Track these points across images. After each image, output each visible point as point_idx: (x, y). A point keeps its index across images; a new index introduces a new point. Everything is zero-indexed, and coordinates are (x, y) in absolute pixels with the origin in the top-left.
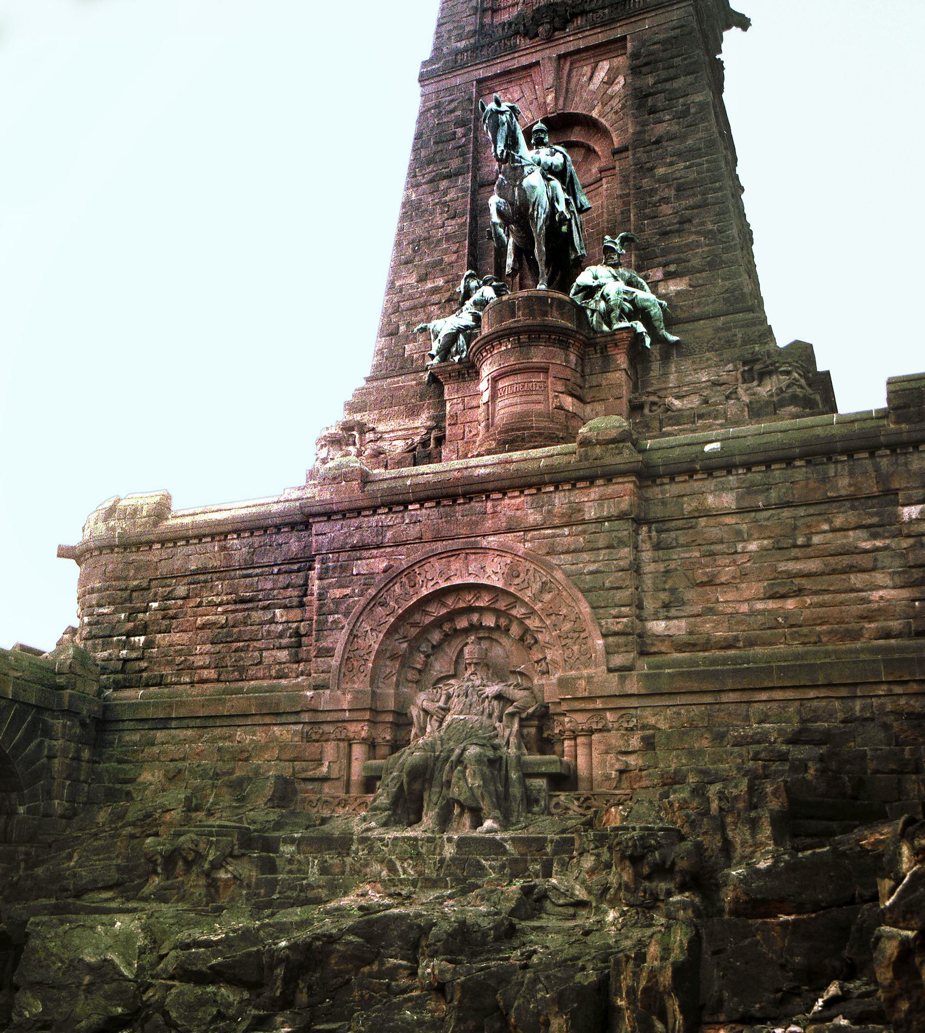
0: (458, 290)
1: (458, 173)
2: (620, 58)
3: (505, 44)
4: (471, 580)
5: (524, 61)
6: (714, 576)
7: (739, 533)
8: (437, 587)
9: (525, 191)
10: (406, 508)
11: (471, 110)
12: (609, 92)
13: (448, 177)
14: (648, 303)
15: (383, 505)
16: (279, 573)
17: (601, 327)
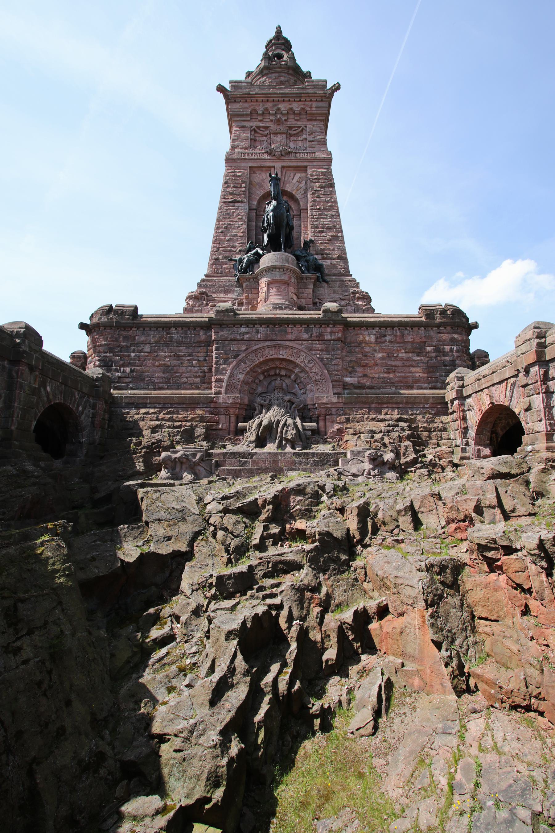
4: (281, 357)
6: (367, 364)
7: (375, 350)
8: (267, 358)
10: (254, 326)
13: (239, 202)
15: (245, 324)
16: (195, 347)
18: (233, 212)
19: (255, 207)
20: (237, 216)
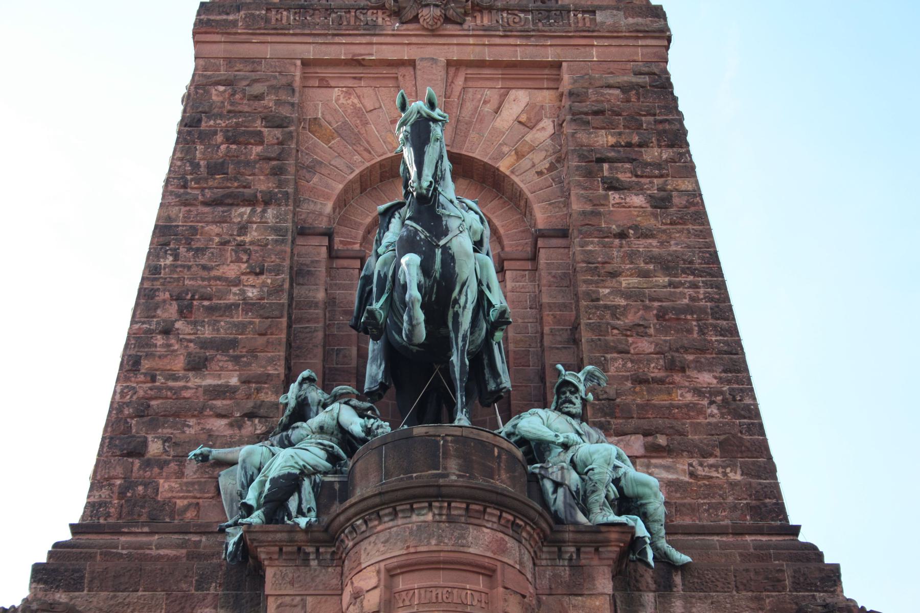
0: (282, 400)
1: (267, 203)
2: (546, 93)
3: (356, 17)
5: (390, 53)
9: (452, 258)
11: (293, 105)
12: (528, 138)
13: (251, 202)
14: (647, 491)
17: (573, 516)
18: (225, 243)
19: (323, 224)
20: (238, 260)
